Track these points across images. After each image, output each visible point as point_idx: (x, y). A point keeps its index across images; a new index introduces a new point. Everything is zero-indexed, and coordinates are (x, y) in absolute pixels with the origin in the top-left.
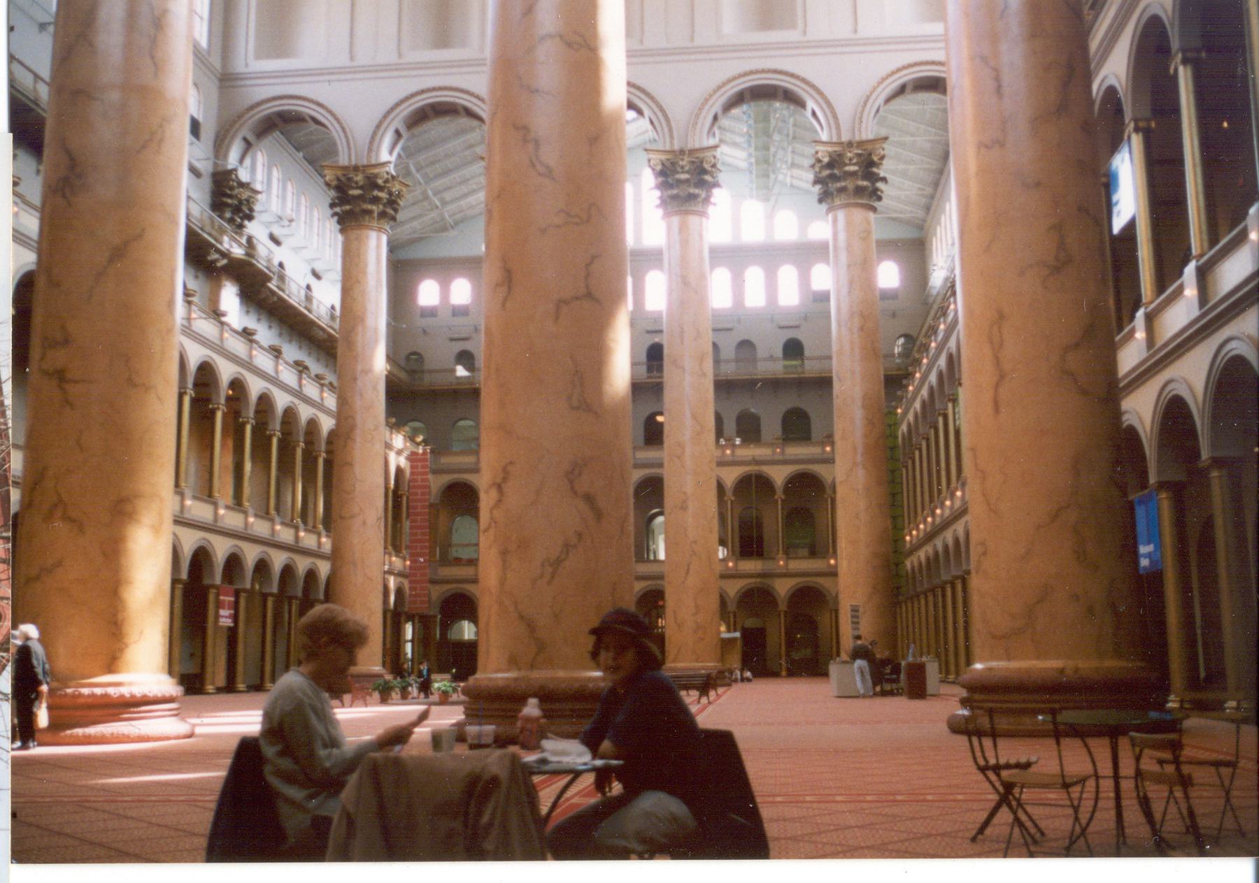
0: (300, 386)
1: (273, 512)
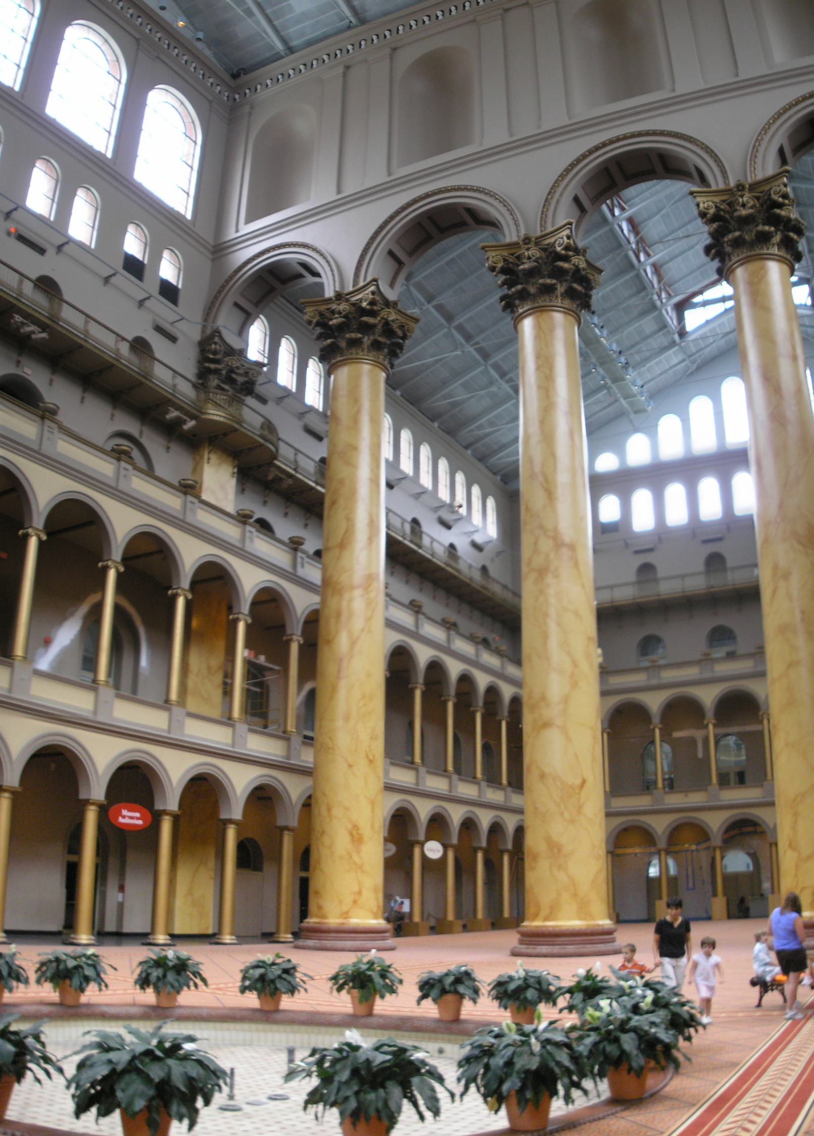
0: (294, 566)
1: (417, 759)
